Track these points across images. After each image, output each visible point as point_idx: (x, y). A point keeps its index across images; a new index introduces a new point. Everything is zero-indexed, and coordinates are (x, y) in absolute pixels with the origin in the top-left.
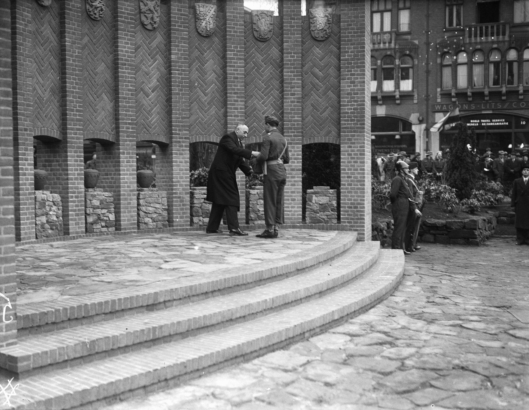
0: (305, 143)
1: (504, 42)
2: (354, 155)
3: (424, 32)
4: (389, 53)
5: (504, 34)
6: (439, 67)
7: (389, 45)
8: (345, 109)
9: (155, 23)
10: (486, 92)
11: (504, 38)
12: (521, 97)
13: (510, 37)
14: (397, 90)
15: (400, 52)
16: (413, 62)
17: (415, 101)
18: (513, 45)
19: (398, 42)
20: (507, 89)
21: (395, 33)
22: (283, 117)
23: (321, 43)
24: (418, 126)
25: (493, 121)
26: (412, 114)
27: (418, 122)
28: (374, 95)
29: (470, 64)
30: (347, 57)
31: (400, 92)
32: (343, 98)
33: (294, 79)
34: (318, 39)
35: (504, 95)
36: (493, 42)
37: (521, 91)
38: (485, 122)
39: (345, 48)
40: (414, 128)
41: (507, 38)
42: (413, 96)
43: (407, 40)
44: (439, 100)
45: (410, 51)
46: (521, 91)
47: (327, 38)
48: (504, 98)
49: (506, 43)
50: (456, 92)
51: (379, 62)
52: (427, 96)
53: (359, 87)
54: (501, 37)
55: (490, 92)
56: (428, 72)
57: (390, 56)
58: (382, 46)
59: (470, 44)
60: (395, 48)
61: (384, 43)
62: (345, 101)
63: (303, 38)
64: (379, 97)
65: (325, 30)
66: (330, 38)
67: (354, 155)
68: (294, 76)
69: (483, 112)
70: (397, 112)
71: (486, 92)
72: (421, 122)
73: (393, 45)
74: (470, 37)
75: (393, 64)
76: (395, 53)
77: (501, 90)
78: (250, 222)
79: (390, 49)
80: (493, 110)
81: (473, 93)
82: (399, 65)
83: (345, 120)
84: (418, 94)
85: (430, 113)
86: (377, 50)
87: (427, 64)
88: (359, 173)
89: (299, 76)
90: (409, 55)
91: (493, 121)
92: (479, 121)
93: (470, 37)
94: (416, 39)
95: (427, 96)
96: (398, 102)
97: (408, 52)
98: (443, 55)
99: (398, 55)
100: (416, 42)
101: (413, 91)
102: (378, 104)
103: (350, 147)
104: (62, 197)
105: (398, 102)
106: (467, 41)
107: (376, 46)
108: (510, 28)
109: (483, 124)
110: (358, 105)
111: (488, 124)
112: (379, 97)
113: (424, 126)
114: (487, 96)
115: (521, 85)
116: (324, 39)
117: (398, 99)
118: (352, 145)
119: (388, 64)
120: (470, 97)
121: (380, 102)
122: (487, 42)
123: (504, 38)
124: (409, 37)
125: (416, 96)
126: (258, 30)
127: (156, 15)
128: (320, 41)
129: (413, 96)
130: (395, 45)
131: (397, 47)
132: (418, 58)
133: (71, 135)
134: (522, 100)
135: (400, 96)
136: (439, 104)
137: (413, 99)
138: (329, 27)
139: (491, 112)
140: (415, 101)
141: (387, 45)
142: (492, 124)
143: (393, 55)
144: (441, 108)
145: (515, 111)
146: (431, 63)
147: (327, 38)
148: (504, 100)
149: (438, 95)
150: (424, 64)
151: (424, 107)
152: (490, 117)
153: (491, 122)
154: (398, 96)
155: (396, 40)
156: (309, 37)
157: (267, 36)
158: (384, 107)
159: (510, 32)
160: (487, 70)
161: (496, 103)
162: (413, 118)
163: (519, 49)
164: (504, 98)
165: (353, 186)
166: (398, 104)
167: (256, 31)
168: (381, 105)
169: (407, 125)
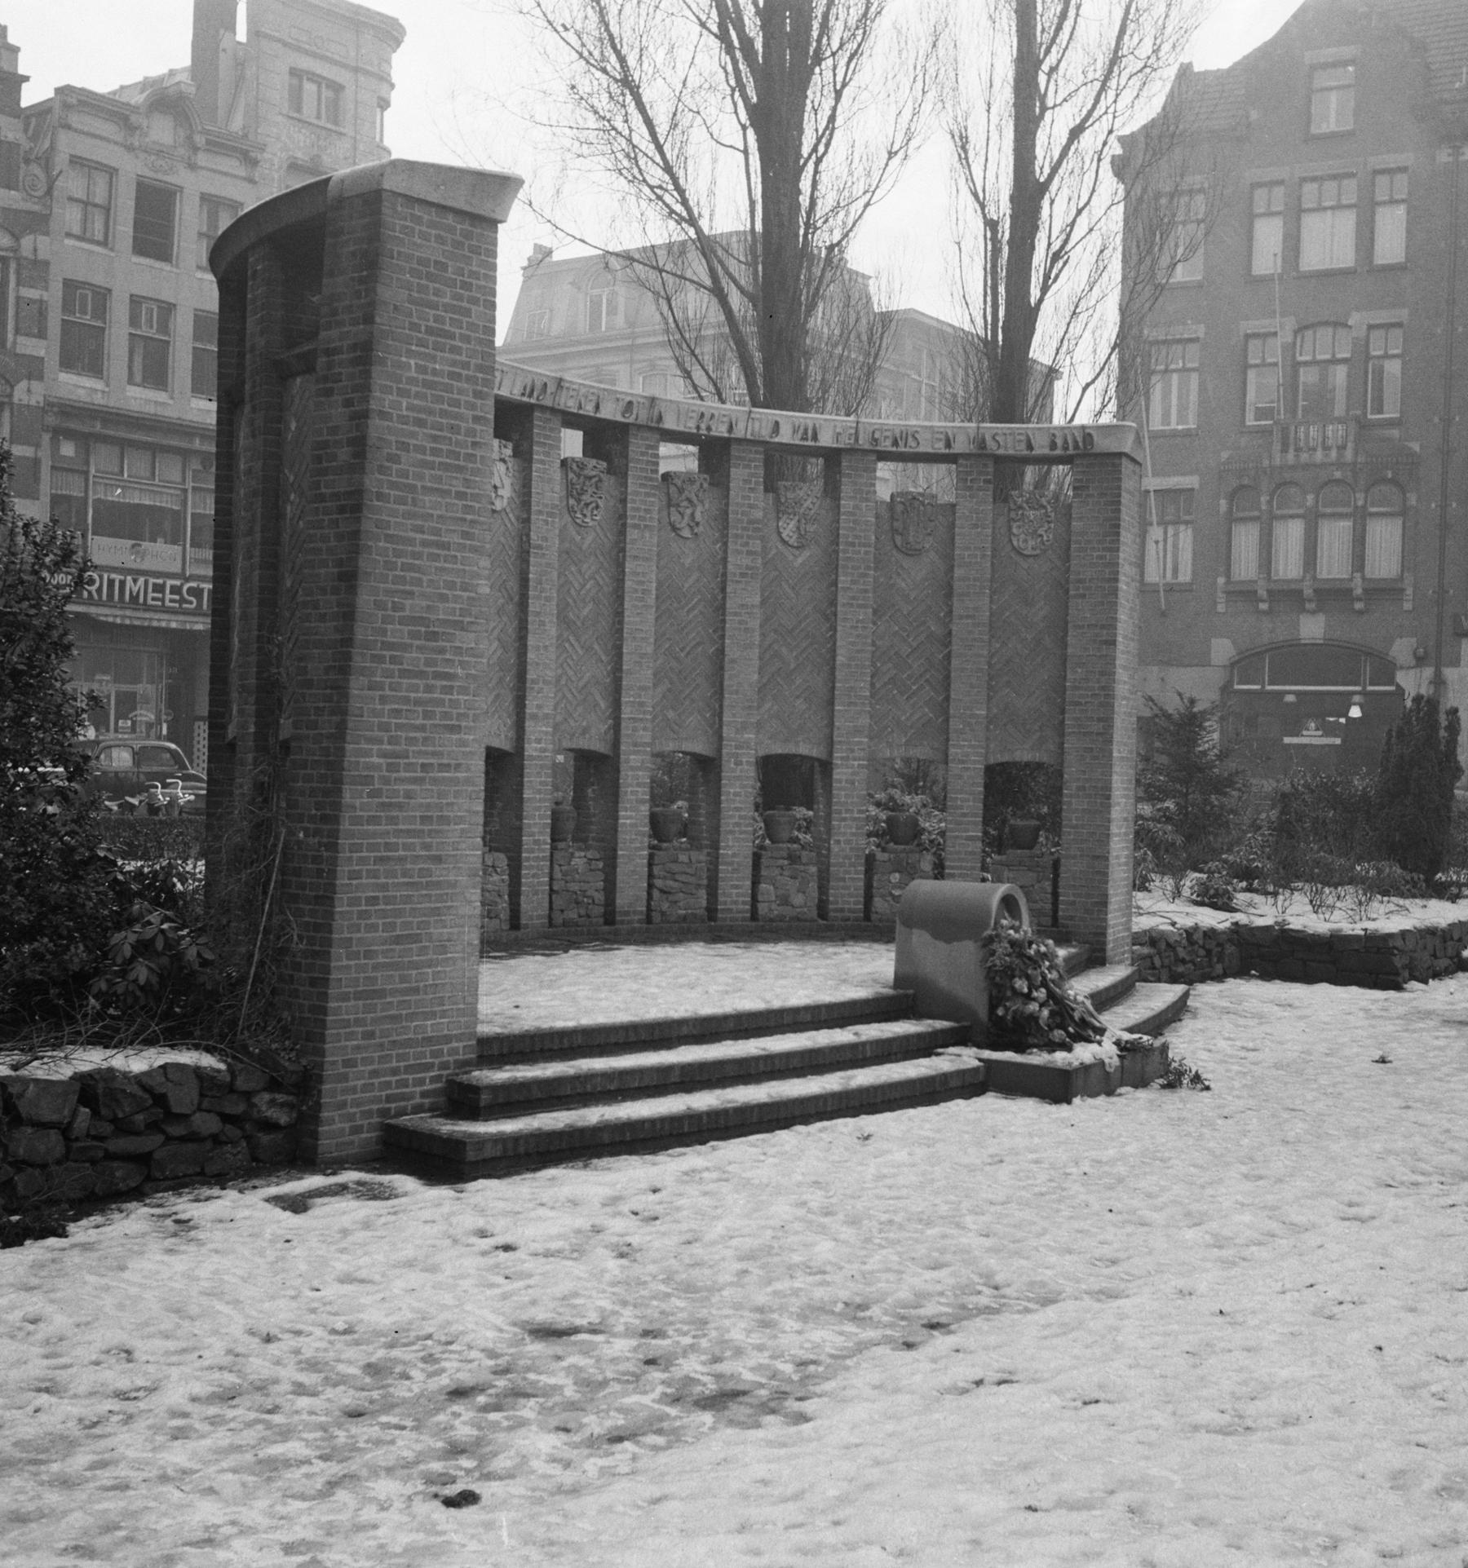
0: (992, 761)
3: (1436, 420)
7: (1340, 455)
9: (697, 524)
14: (1358, 575)
16: (1405, 500)
17: (1407, 606)
21: (1357, 420)
24: (1412, 672)
26: (1398, 641)
27: (1414, 663)
31: (1363, 578)
51: (1310, 498)
58: (1319, 456)
60: (1355, 463)
61: (1326, 448)
64: (1308, 592)
72: (1420, 661)
73: (1349, 455)
79: (1340, 465)
82: (1364, 507)
84: (1415, 588)
86: (1306, 467)
87: (1444, 507)
90: (1394, 482)
96: (1358, 606)
100: (1416, 447)
101: (1401, 578)
102: (1304, 610)
104: (509, 859)
105: (1358, 606)
107: (1304, 457)
112: (1308, 592)
113: (1428, 672)
121: (1308, 606)
124: (1395, 433)
125: (1409, 591)
127: (699, 509)
128: (1028, 556)
129: (1403, 590)
130: (1356, 453)
133: (531, 749)
135: (1365, 590)
140: (1407, 606)
141: (1334, 454)
147: (1045, 551)
154: (1359, 591)
158: (1321, 618)
162: (1402, 649)
166: (1361, 612)
168: (1313, 612)
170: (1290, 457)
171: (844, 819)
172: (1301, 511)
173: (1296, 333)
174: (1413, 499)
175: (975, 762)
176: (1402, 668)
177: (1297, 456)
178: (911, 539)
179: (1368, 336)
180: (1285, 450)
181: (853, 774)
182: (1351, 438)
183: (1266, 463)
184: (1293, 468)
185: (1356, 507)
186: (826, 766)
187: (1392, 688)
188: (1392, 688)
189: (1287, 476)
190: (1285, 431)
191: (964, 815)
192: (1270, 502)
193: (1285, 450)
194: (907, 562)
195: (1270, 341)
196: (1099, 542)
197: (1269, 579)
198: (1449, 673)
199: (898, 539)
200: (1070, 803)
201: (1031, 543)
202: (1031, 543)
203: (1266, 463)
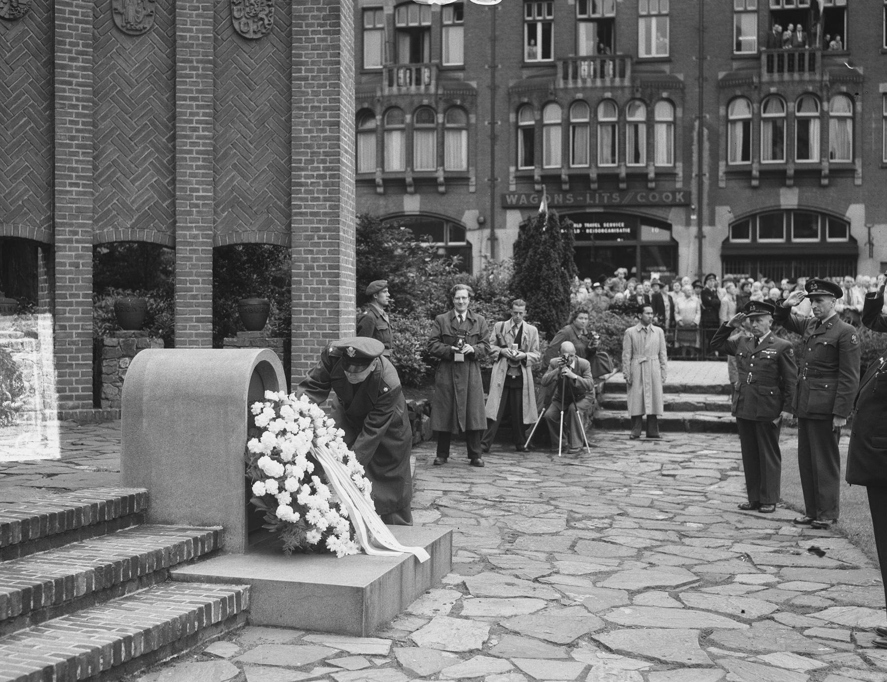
1: (622, 88)
2: (319, 267)
3: (486, 67)
4: (426, 102)
5: (622, 76)
6: (512, 130)
8: (300, 177)
10: (593, 175)
11: (622, 81)
12: (652, 185)
13: (633, 79)
14: (441, 168)
15: (446, 101)
16: (468, 119)
17: (472, 189)
18: (638, 95)
19: (444, 82)
20: (629, 171)
22: (174, 189)
23: (254, 44)
24: (477, 233)
25: (605, 225)
26: (467, 212)
27: (477, 226)
28: (400, 176)
29: (567, 126)
30: (303, 74)
31: (445, 171)
32: (299, 154)
33: (197, 114)
34: (247, 36)
35: (623, 181)
36: (604, 89)
37: (652, 175)
38: (592, 228)
39: (300, 56)
40: (471, 237)
41: (627, 82)
42: (468, 179)
43: (458, 79)
44: (513, 188)
45: (463, 100)
46: (652, 175)
47: (265, 35)
48: (623, 186)
49: (627, 91)
50: (543, 174)
51: (408, 118)
52: (493, 179)
53: (328, 134)
54: (617, 79)
55: (599, 176)
56: (493, 138)
57: (428, 106)
59: (566, 89)
60: (436, 94)
62: (300, 161)
63: (216, 32)
64: (409, 180)
65: (262, 19)
66: (272, 36)
67: (319, 267)
68: (198, 107)
69: (588, 210)
70: (441, 206)
71: (593, 175)
72: (482, 225)
73: (432, 89)
74: (565, 78)
75: (433, 122)
76: (437, 103)
77: (617, 171)
78: (104, 403)
79: (427, 95)
80: (605, 207)
81: (570, 176)
82: (443, 124)
83: (301, 199)
84: (476, 177)
85: (498, 209)
87: (493, 123)
88: (326, 305)
89: (208, 106)
90: (461, 107)
91: (605, 225)
92: (580, 225)
93: (565, 78)
94: (473, 79)
95: (493, 179)
96: (442, 189)
97: (459, 102)
98: (520, 108)
99: (442, 106)
100: (474, 84)
101: (468, 171)
102: (406, 192)
103: (311, 252)
106: (561, 84)
107: (404, 89)
108: (632, 65)
109: (587, 231)
110: (326, 169)
111: (596, 231)
112: (409, 180)
113: (487, 232)
114: (594, 182)
115: (652, 163)
116: (259, 36)
117: (441, 185)
118: (315, 249)
119: (424, 122)
120: (565, 183)
122: (593, 89)
123: (622, 81)
124: (461, 75)
125: (473, 179)
126: (121, 11)
128: (252, 40)
131: (440, 92)
132: (476, 114)
134: (652, 189)
135: (445, 179)
136: (513, 193)
137: (468, 185)
138: (270, 12)
139: (601, 210)
140: (472, 189)
142: (603, 231)
143: (434, 105)
144: (518, 199)
145: (644, 210)
146: (499, 123)
147: (265, 35)
148: (623, 190)
149: (511, 178)
150: (486, 123)
151: (487, 199)
152: (601, 219)
153: (602, 227)
154: (441, 179)
155: (438, 79)
156: (229, 32)
157: (141, 26)
159: (633, 72)
160: (594, 135)
161: (611, 194)
162: (469, 218)
163: (648, 102)
164: (623, 186)
165: (315, 331)
166: (443, 194)
167: (121, 14)
168: (412, 194)
169: (459, 232)
170: (395, 89)
171: (70, 304)
172: (402, 126)
173: (396, 7)
174: (473, 119)
175: (203, 244)
176: (470, 230)
177: (399, 90)
178: (131, 19)
179: (441, 13)
180: (391, 85)
181: (78, 257)
182: (434, 77)
183: (379, 94)
184: (396, 96)
185: (438, 123)
186: (49, 249)
187: (464, 244)
188: (464, 244)
189: (393, 102)
190: (390, 71)
191: (194, 297)
192: (383, 120)
193: (391, 85)
194: (128, 44)
195: (378, 13)
196: (320, 25)
197: (383, 172)
198: (499, 233)
199: (118, 20)
200: (300, 282)
201: (253, 27)
202: (253, 27)
203: (379, 94)
